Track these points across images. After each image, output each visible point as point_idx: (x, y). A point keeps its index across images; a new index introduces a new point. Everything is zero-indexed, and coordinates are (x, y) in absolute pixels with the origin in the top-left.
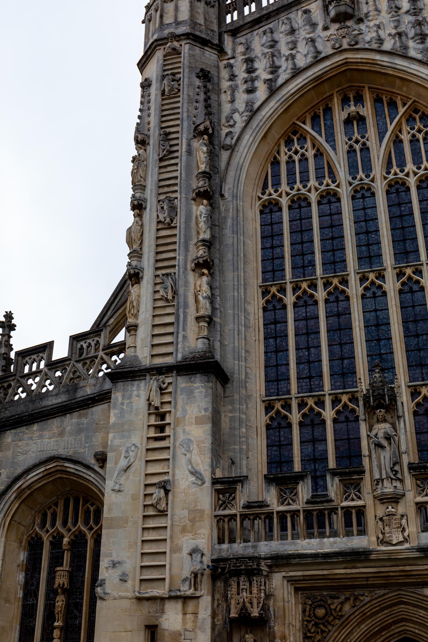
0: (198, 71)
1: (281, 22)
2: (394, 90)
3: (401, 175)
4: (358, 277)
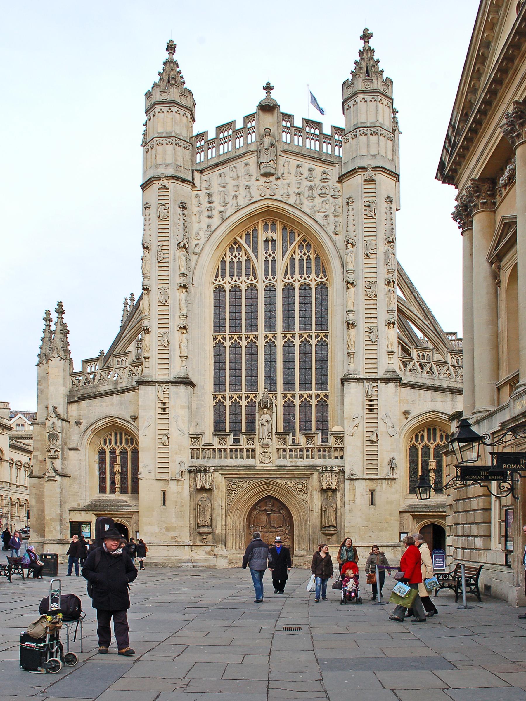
3: (291, 281)
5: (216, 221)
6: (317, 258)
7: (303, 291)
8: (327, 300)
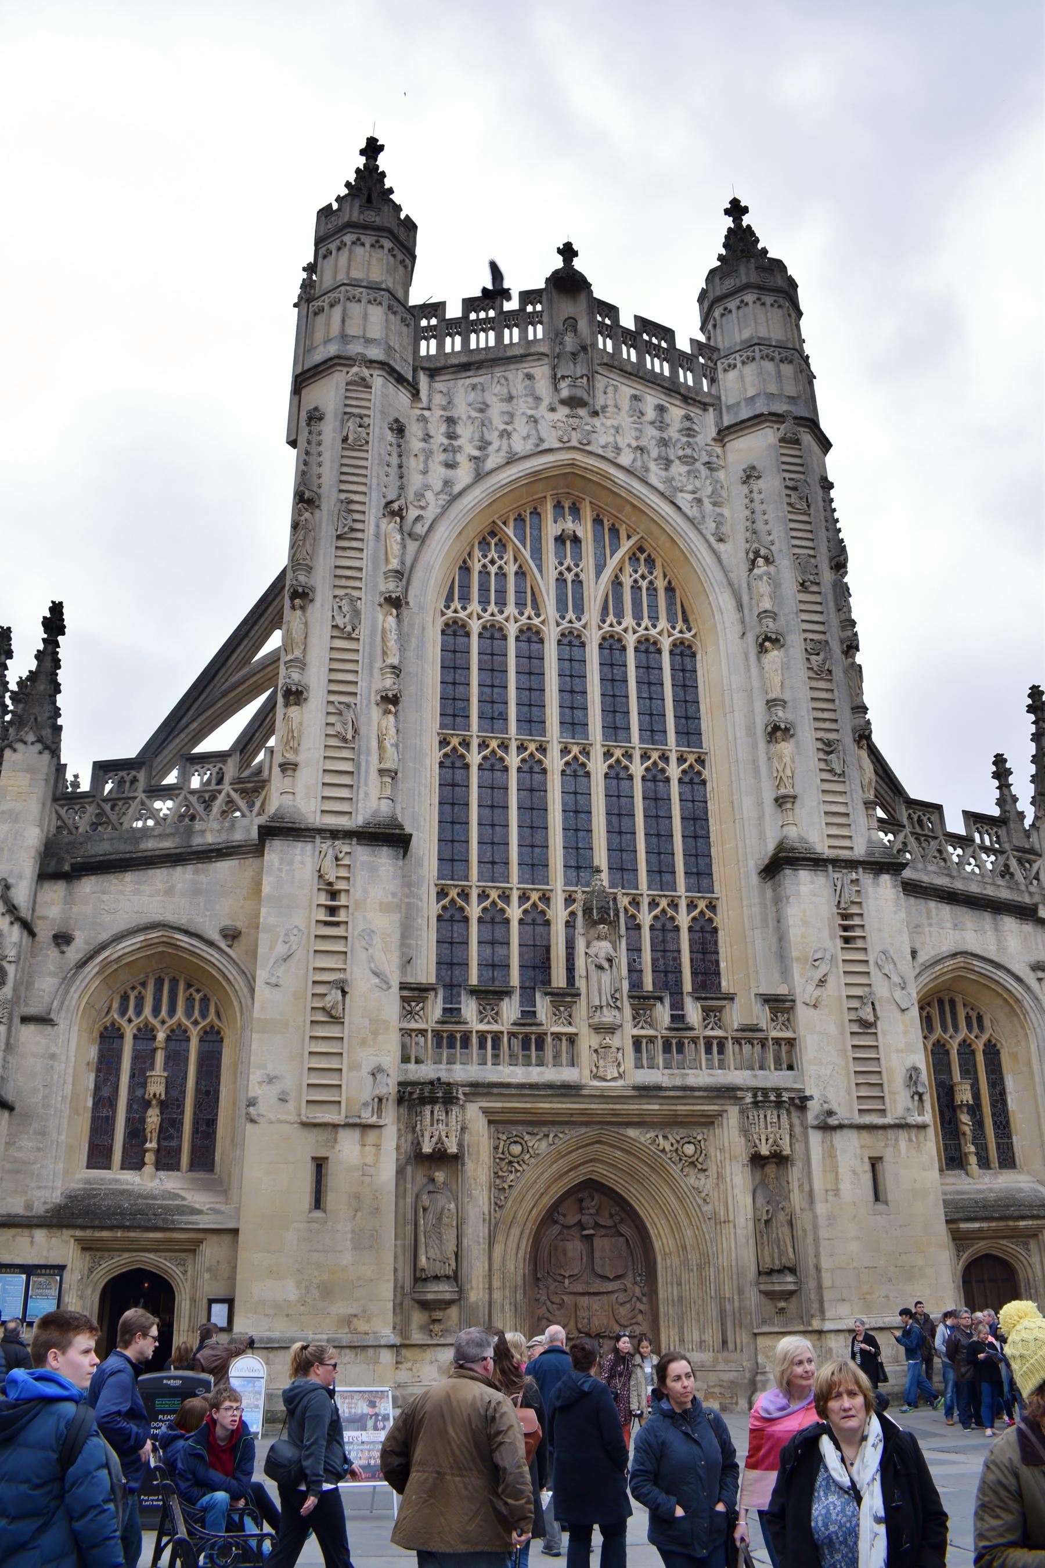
0: (391, 419)
1: (496, 380)
2: (620, 516)
4: (560, 746)
5: (463, 475)
6: (670, 589)
7: (643, 656)
8: (696, 680)
